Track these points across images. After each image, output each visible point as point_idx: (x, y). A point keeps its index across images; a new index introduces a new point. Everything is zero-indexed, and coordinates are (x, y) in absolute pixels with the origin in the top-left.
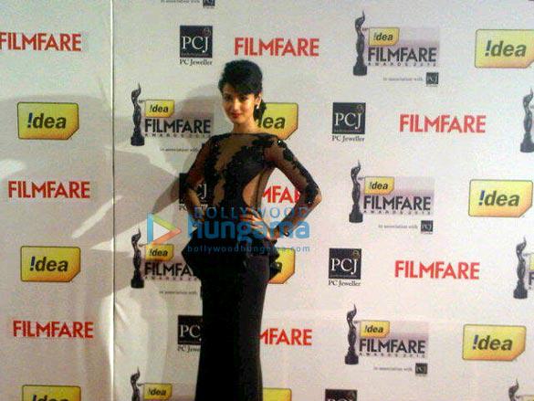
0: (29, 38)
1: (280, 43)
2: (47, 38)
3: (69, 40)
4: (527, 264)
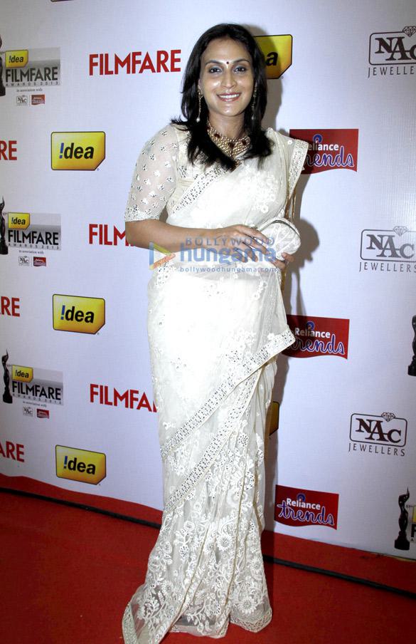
0: (122, 61)
1: (135, 396)
2: (141, 58)
3: (166, 59)
4: (410, 515)
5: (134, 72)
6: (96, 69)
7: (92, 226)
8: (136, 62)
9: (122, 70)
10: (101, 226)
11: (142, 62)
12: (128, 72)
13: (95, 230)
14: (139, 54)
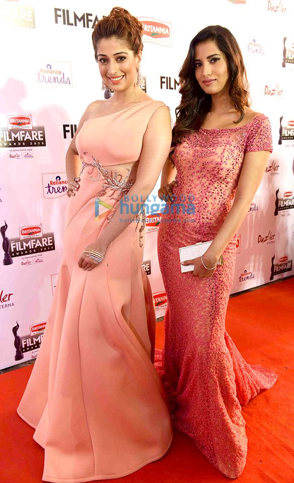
0: (80, 17)
5: (88, 27)
6: (60, 20)
7: (65, 126)
8: (89, 20)
9: (80, 24)
10: (72, 126)
11: (93, 21)
12: (84, 26)
13: (67, 128)
14: (91, 15)
